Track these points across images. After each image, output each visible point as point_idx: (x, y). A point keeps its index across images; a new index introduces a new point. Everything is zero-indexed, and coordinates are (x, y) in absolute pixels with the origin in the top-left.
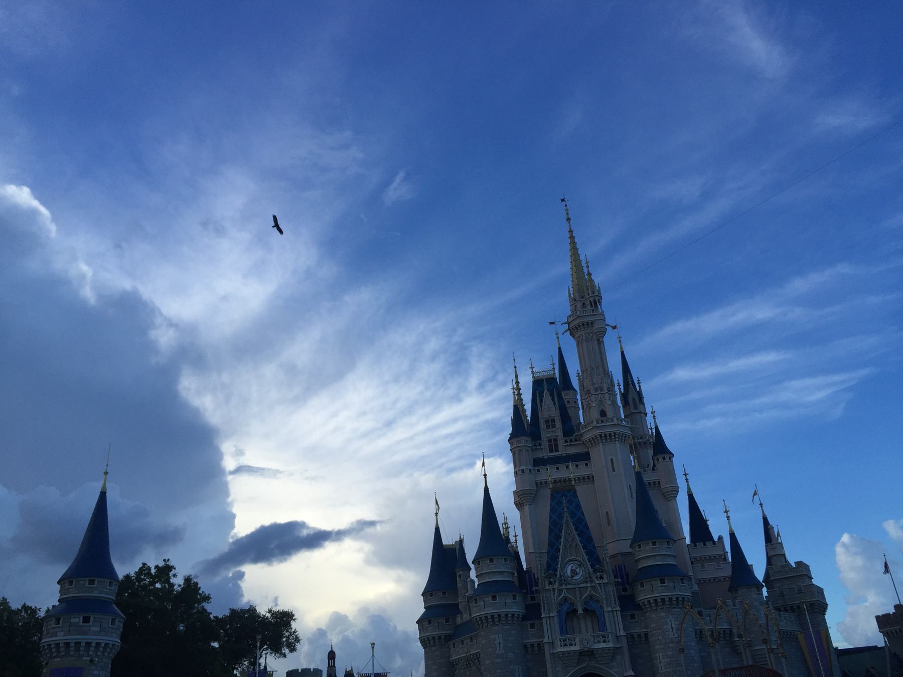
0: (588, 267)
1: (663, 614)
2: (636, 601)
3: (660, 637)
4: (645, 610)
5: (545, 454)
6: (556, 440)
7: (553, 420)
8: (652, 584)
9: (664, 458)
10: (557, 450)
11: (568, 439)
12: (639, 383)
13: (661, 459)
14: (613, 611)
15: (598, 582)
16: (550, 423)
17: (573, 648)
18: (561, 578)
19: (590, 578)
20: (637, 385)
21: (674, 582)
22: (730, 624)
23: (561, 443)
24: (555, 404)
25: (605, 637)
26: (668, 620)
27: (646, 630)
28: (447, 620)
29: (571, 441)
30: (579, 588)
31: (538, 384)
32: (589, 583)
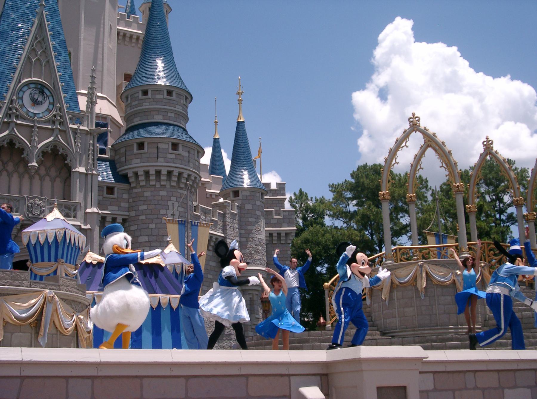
1: (163, 193)
2: (118, 170)
3: (152, 226)
4: (133, 185)
8: (158, 147)
14: (86, 174)
15: (75, 127)
18: (11, 103)
19: (60, 117)
21: (189, 152)
22: (224, 231)
25: (70, 209)
26: (170, 203)
27: (127, 213)
30: (38, 127)
32: (57, 123)
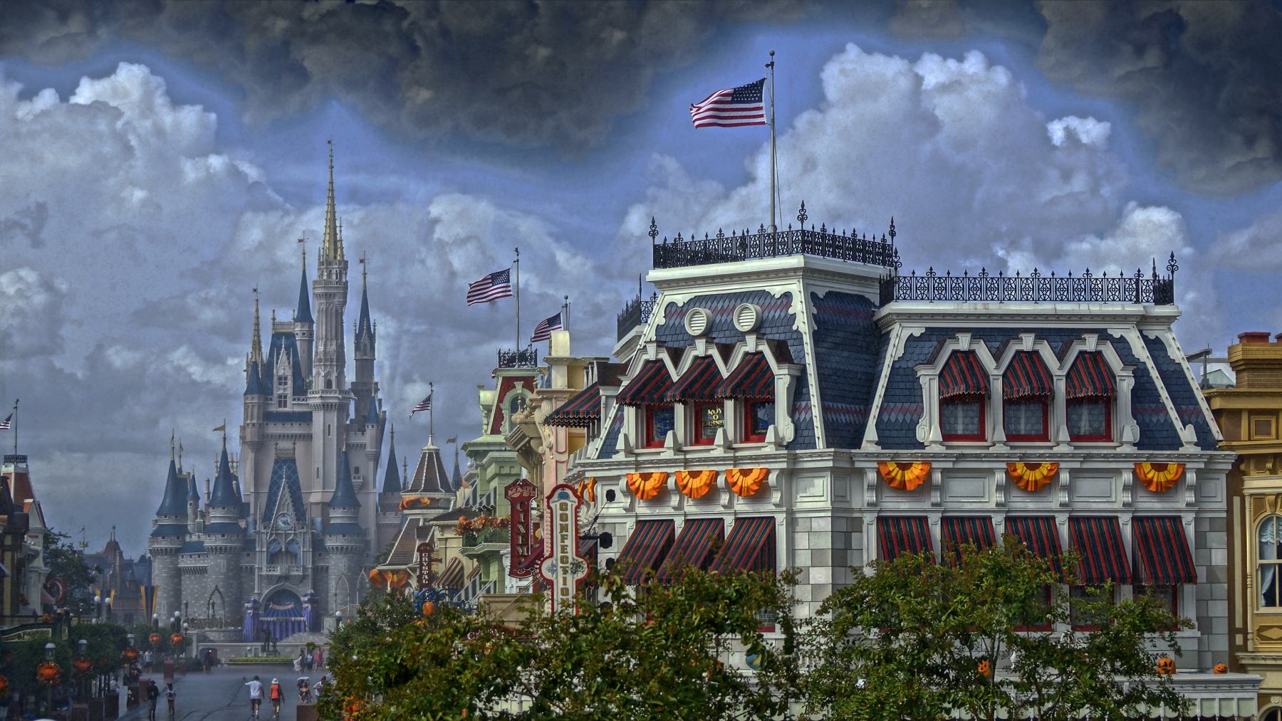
0: (341, 231)
5: (274, 408)
6: (285, 397)
7: (286, 378)
9: (373, 427)
10: (285, 406)
11: (296, 397)
12: (375, 326)
13: (370, 427)
16: (282, 380)
17: (275, 573)
20: (372, 328)
23: (290, 401)
24: (289, 363)
28: (178, 538)
29: (299, 400)
31: (276, 337)
